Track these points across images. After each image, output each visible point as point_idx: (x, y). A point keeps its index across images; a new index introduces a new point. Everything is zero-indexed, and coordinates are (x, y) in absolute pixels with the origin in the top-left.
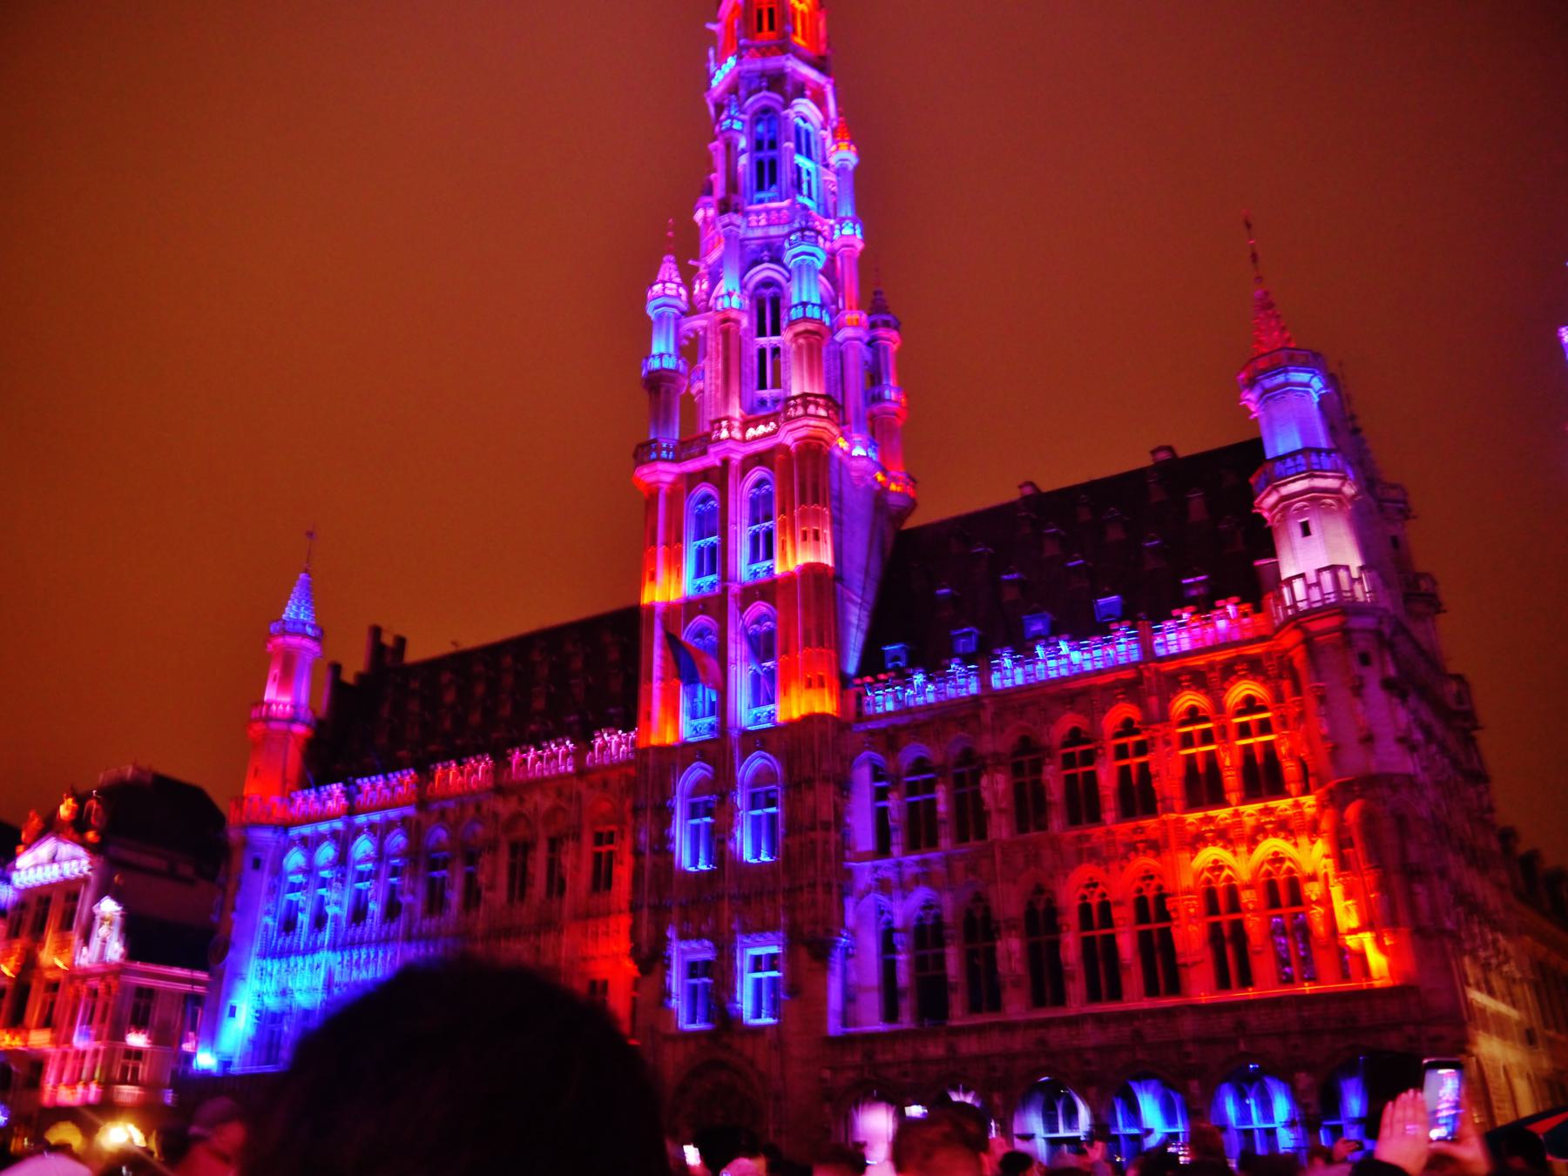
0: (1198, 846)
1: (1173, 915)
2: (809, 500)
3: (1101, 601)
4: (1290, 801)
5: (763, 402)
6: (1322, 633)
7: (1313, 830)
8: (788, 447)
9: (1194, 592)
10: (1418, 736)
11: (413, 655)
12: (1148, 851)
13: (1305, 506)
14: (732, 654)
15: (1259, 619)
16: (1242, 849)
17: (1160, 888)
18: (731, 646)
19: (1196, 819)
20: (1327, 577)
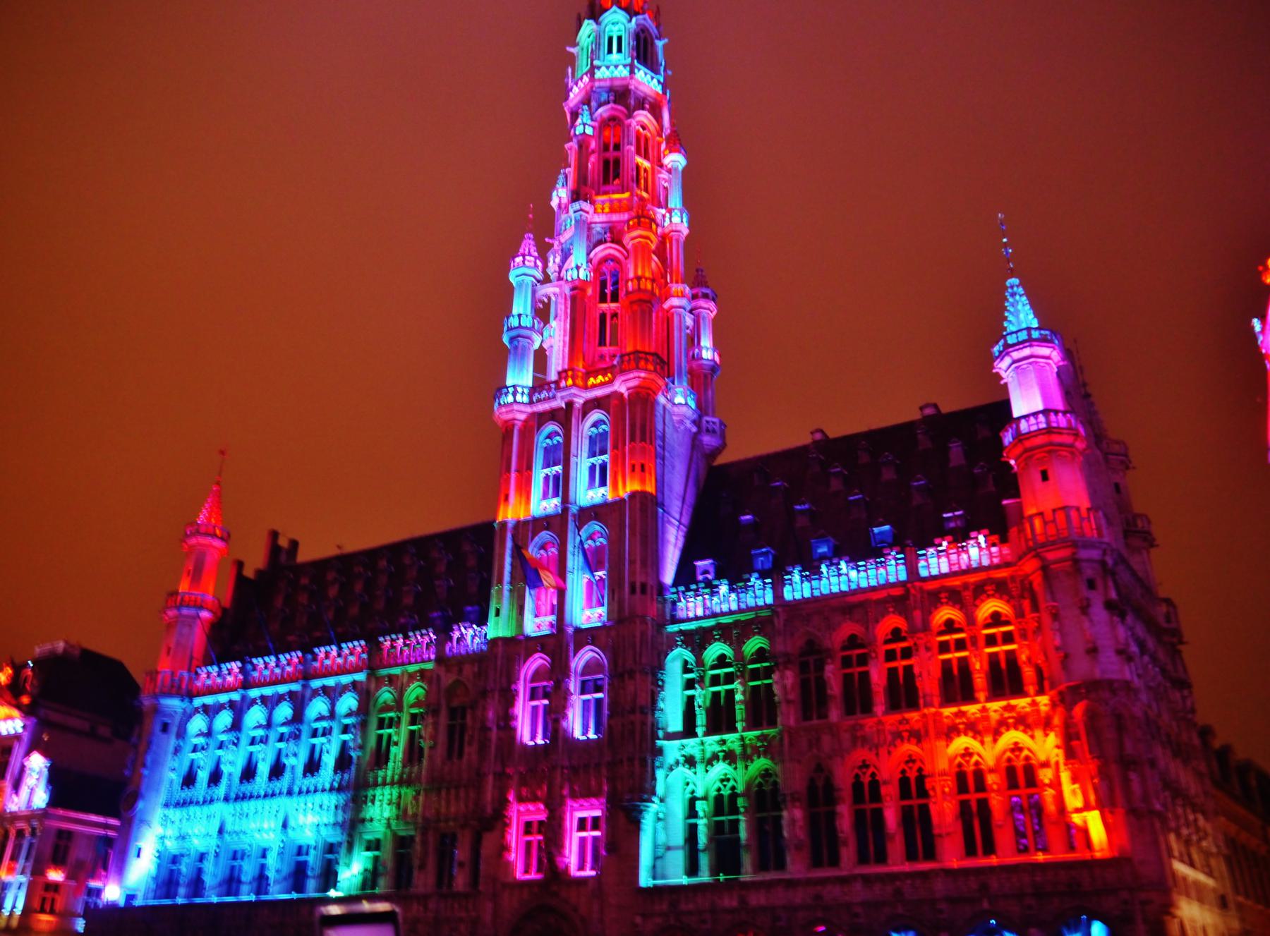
0: (952, 735)
1: (931, 793)
2: (638, 439)
3: (876, 530)
4: (1028, 700)
5: (602, 357)
6: (1056, 562)
7: (1046, 725)
8: (622, 395)
9: (952, 525)
10: (1134, 649)
11: (303, 556)
13: (1045, 457)
14: (570, 564)
15: (1006, 551)
16: (988, 739)
17: (920, 770)
18: (570, 557)
19: (951, 713)
20: (1061, 516)
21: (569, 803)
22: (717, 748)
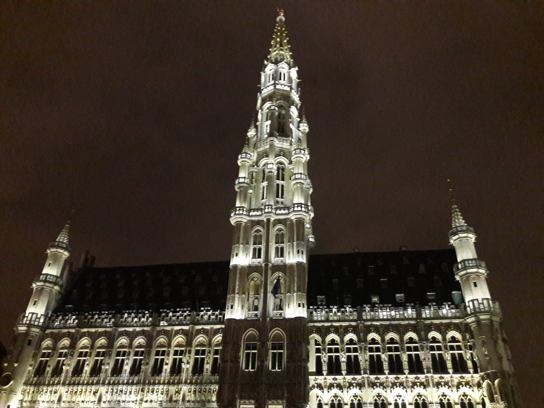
0: (439, 387)
5: (278, 202)
6: (484, 320)
8: (292, 220)
16: (455, 389)
18: (268, 286)
22: (334, 382)
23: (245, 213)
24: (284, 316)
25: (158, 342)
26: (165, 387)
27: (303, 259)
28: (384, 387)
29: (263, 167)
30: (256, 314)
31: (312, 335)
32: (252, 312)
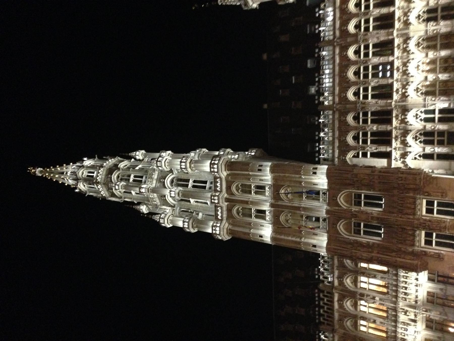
5: (210, 188)
8: (228, 175)
12: (408, 42)
14: (297, 205)
18: (294, 205)
21: (417, 217)
23: (218, 225)
24: (326, 190)
25: (350, 328)
26: (400, 326)
27: (267, 166)
28: (407, 84)
29: (175, 201)
30: (323, 220)
31: (348, 160)
32: (321, 224)
